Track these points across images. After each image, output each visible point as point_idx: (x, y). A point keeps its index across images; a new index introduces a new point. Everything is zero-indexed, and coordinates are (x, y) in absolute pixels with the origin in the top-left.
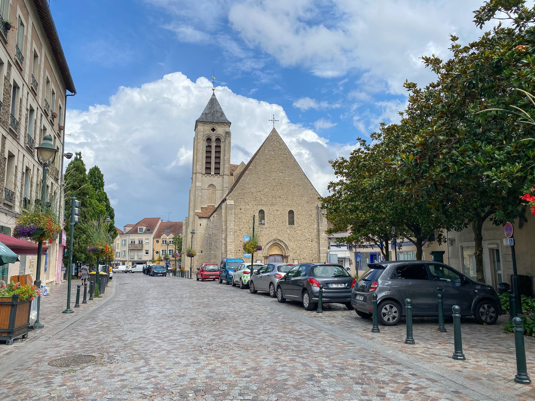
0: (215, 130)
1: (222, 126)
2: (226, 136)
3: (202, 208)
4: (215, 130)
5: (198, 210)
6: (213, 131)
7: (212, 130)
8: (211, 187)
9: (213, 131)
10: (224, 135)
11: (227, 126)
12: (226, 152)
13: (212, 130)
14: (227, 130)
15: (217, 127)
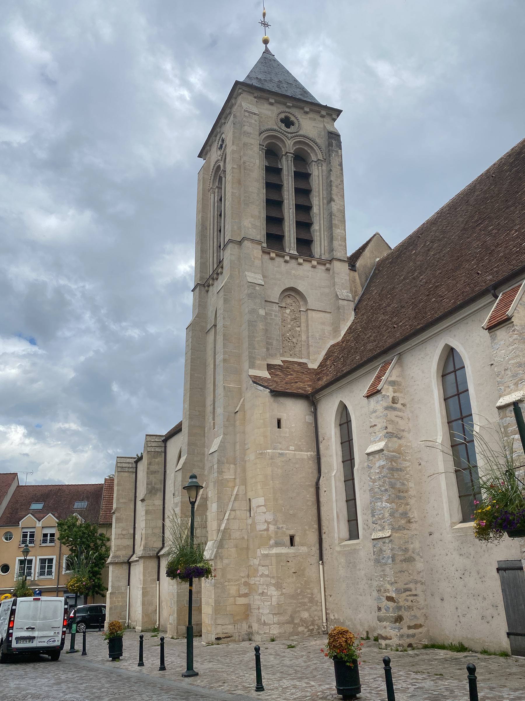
0: (293, 124)
1: (311, 115)
2: (330, 145)
3: (270, 367)
4: (293, 124)
5: (260, 369)
6: (288, 126)
7: (282, 121)
8: (289, 301)
9: (288, 126)
10: (322, 141)
11: (327, 119)
12: (334, 188)
13: (282, 121)
14: (329, 128)
15: (299, 117)
